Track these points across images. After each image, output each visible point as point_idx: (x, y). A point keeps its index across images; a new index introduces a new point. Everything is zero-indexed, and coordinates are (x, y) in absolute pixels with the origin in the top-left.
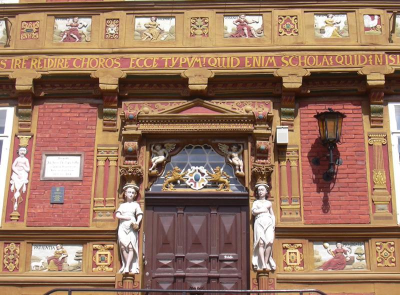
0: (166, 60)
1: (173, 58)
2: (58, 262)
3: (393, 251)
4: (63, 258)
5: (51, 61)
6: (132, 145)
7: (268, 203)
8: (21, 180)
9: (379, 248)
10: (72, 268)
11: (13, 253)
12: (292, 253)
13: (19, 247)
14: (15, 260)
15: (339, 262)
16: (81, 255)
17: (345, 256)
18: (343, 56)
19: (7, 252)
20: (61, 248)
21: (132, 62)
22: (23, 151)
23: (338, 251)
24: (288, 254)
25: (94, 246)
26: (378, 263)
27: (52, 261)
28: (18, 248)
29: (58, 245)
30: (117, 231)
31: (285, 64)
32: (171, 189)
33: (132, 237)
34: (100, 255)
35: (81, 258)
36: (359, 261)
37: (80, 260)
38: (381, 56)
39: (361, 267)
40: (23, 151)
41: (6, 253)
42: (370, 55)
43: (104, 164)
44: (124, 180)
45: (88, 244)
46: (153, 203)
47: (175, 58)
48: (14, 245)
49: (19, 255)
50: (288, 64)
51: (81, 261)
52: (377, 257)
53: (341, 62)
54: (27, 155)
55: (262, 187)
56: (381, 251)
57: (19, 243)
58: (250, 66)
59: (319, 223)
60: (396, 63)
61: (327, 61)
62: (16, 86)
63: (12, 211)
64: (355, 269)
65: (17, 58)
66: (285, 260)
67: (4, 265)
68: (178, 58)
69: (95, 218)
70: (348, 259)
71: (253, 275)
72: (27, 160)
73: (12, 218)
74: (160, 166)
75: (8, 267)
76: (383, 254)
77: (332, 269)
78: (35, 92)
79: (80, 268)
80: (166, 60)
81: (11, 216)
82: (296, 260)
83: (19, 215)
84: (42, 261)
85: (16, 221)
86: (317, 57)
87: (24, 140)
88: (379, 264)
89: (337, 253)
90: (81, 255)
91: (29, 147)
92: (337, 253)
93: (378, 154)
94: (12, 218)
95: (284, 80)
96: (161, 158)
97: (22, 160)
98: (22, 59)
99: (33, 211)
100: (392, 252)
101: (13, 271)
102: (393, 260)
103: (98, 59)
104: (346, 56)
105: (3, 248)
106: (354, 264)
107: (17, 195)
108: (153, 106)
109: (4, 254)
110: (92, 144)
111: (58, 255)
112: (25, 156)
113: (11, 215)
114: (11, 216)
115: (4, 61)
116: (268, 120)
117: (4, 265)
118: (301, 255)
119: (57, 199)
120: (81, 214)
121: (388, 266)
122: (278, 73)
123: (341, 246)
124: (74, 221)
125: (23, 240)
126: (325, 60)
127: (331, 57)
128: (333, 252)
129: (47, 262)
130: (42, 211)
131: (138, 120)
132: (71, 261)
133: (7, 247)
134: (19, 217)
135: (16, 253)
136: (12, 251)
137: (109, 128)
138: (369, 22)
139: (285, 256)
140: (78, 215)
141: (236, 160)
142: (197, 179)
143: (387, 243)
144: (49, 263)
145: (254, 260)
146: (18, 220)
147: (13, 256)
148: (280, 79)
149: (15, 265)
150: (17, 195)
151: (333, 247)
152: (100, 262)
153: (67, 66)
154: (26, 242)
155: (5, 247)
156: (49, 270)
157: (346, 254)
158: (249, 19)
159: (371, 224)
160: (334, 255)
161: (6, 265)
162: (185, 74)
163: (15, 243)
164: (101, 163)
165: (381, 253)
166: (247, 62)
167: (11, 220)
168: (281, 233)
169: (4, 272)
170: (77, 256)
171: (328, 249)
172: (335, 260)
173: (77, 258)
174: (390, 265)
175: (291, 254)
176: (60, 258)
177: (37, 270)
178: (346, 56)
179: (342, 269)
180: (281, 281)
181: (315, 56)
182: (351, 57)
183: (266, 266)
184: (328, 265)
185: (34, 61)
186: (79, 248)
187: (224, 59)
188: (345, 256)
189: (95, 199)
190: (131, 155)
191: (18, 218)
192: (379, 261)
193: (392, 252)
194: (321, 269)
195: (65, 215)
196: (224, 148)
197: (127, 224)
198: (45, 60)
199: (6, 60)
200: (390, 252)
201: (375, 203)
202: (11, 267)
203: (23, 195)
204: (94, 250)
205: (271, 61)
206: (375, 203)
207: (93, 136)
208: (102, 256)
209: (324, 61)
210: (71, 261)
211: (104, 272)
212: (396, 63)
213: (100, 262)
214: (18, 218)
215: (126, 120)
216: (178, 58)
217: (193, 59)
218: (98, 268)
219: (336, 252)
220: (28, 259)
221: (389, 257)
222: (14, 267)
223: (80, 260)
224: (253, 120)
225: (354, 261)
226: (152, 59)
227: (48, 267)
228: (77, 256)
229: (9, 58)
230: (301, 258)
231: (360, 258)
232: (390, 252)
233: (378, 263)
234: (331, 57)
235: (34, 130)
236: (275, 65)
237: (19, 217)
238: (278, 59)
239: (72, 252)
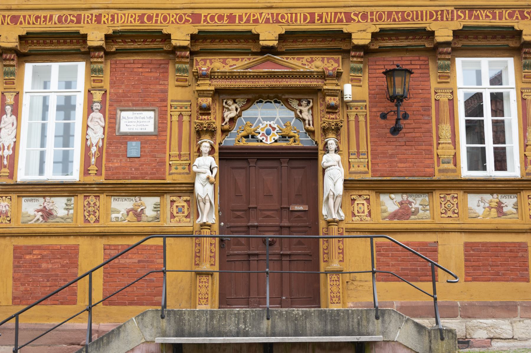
0: (237, 16)
1: (244, 14)
2: (138, 215)
3: (457, 202)
4: (142, 209)
5: (121, 16)
6: (206, 101)
7: (337, 157)
9: (443, 200)
10: (151, 219)
11: (93, 205)
12: (360, 203)
13: (99, 200)
14: (96, 212)
16: (159, 206)
17: (410, 207)
18: (412, 12)
19: (87, 205)
20: (140, 200)
21: (203, 18)
22: (97, 106)
23: (403, 203)
24: (356, 205)
25: (172, 198)
26: (442, 213)
27: (131, 213)
28: (98, 201)
29: (137, 198)
30: (193, 184)
31: (354, 20)
32: (244, 143)
33: (210, 188)
34: (177, 206)
35: (158, 209)
36: (423, 212)
37: (157, 211)
38: (450, 11)
39: (425, 218)
40: (97, 106)
41: (86, 206)
42: (438, 11)
43: (178, 120)
45: (165, 195)
47: (246, 14)
48: (94, 198)
49: (99, 207)
50: (357, 21)
51: (159, 212)
52: (441, 208)
53: (409, 18)
54: (102, 111)
55: (332, 143)
56: (444, 203)
57: (99, 196)
58: (320, 22)
59: (386, 175)
60: (465, 19)
61: (396, 17)
62: (88, 42)
63: (90, 166)
64: (419, 219)
65: (87, 13)
66: (353, 210)
67: (85, 216)
68: (248, 14)
69: (171, 172)
70: (413, 209)
72: (100, 115)
73: (90, 172)
74: (232, 120)
75: (89, 219)
76: (446, 205)
77: (398, 219)
78: (106, 46)
79: (158, 219)
80: (237, 16)
81: (89, 170)
82: (364, 210)
83: (97, 169)
84: (121, 213)
85: (94, 175)
86: (386, 13)
87: (98, 96)
88: (443, 215)
89: (402, 204)
90: (159, 206)
91: (103, 102)
92: (402, 204)
93: (446, 109)
94: (90, 172)
95: (354, 36)
96: (233, 114)
97: (97, 115)
98: (92, 15)
99: (111, 165)
100: (455, 203)
101: (94, 222)
102: (456, 211)
103: (169, 14)
104: (415, 13)
105: (83, 201)
106: (419, 214)
107: (94, 150)
108: (224, 62)
109: (84, 206)
110: (164, 100)
111: (137, 207)
112: (100, 111)
113: (88, 169)
114: (89, 170)
115: (73, 16)
116: (339, 75)
117: (85, 216)
118: (368, 206)
120: (157, 167)
121: (451, 217)
122: (346, 29)
123: (406, 198)
124: (151, 174)
125: (103, 193)
126: (394, 16)
127: (400, 13)
128: (399, 203)
129: (126, 213)
130: (119, 165)
131: (211, 76)
132: (149, 212)
133: (87, 200)
134: (97, 170)
135: (96, 205)
136: (92, 203)
137: (182, 83)
139: (353, 207)
140: (155, 168)
141: (306, 115)
142: (268, 133)
143: (452, 195)
144: (128, 215)
146: (96, 174)
147: (93, 208)
148: (349, 36)
149: (95, 217)
150: (94, 150)
151: (398, 198)
152: (177, 213)
153: (138, 21)
154: (105, 194)
155: (85, 200)
156: (129, 221)
157: (411, 205)
159: (436, 177)
160: (400, 206)
161: (87, 217)
162: (255, 29)
163: (94, 196)
164: (175, 118)
165: (445, 204)
166: (317, 18)
167: (90, 174)
169: (86, 224)
170: (155, 208)
171: (395, 200)
172: (401, 210)
173: (156, 209)
174: (452, 216)
175: (360, 205)
176: (139, 210)
177: (117, 221)
178: (415, 13)
179: (407, 219)
181: (384, 12)
182: (419, 12)
183: (335, 216)
184: (394, 216)
185: (105, 16)
186: (157, 200)
187: (294, 15)
188: (410, 207)
189: (170, 153)
190: (205, 111)
191: (96, 172)
192: (442, 212)
193: (455, 203)
194: (387, 219)
195: (142, 168)
196: (295, 104)
197: (204, 176)
198: (116, 16)
199: (76, 15)
200: (453, 204)
201: (439, 157)
202: (92, 218)
203: (100, 150)
204: (171, 201)
205: (341, 18)
206: (439, 157)
207: (165, 92)
208: (179, 207)
209: (393, 17)
210: (149, 212)
212: (465, 19)
213: (177, 213)
214: (96, 172)
215: (199, 76)
216: (248, 14)
217: (263, 15)
218: (175, 219)
219: (401, 203)
220: (109, 211)
221: (453, 208)
222: (95, 219)
223: (157, 211)
224: (323, 76)
225: (418, 212)
226: (223, 15)
227: (127, 219)
228: (155, 208)
229: (79, 13)
230: (368, 209)
231: (424, 209)
232: (453, 204)
233: (442, 213)
234: (400, 13)
235: (107, 86)
236: (345, 21)
237: (97, 170)
238: (347, 15)
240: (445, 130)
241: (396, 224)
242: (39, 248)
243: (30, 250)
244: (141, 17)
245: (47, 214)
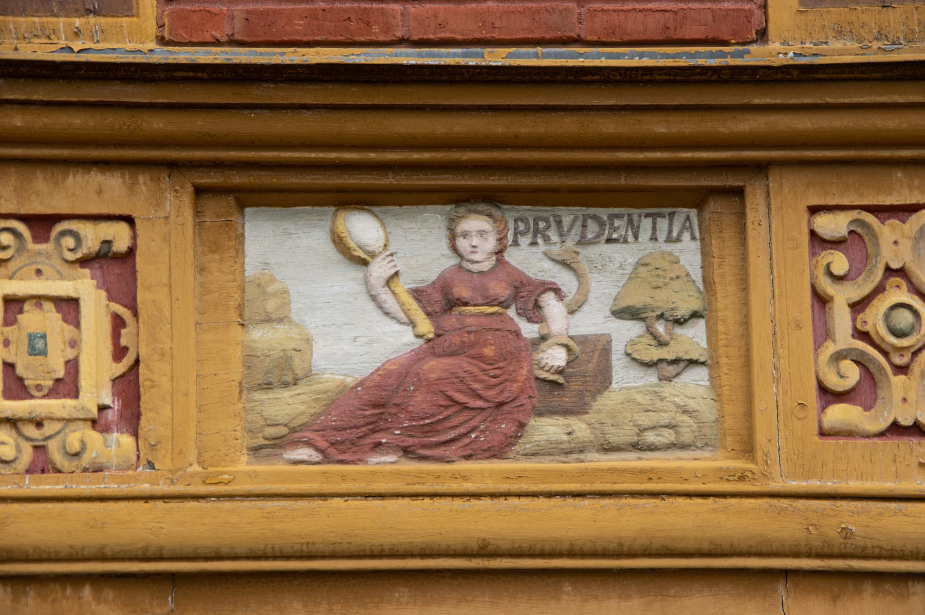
9: (840, 262)
12: (39, 299)
17: (529, 330)
23: (460, 291)
26: (828, 395)
36: (651, 378)
39: (668, 436)
52: (818, 346)
56: (855, 292)
64: (609, 448)
70: (556, 357)
76: (874, 318)
77: (407, 452)
82: (73, 366)
88: (838, 414)
89: (452, 303)
92: (452, 303)
106: (608, 401)
118: (118, 323)
123: (491, 244)
128: (418, 294)
157: (534, 313)
159: (774, 46)
160: (426, 327)
165: (858, 307)
171: (380, 270)
172: (434, 367)
179: (497, 452)
188: (529, 330)
192: (834, 382)
194: (304, 453)
225: (604, 378)
230: (119, 353)
231: (655, 354)
233: (828, 395)
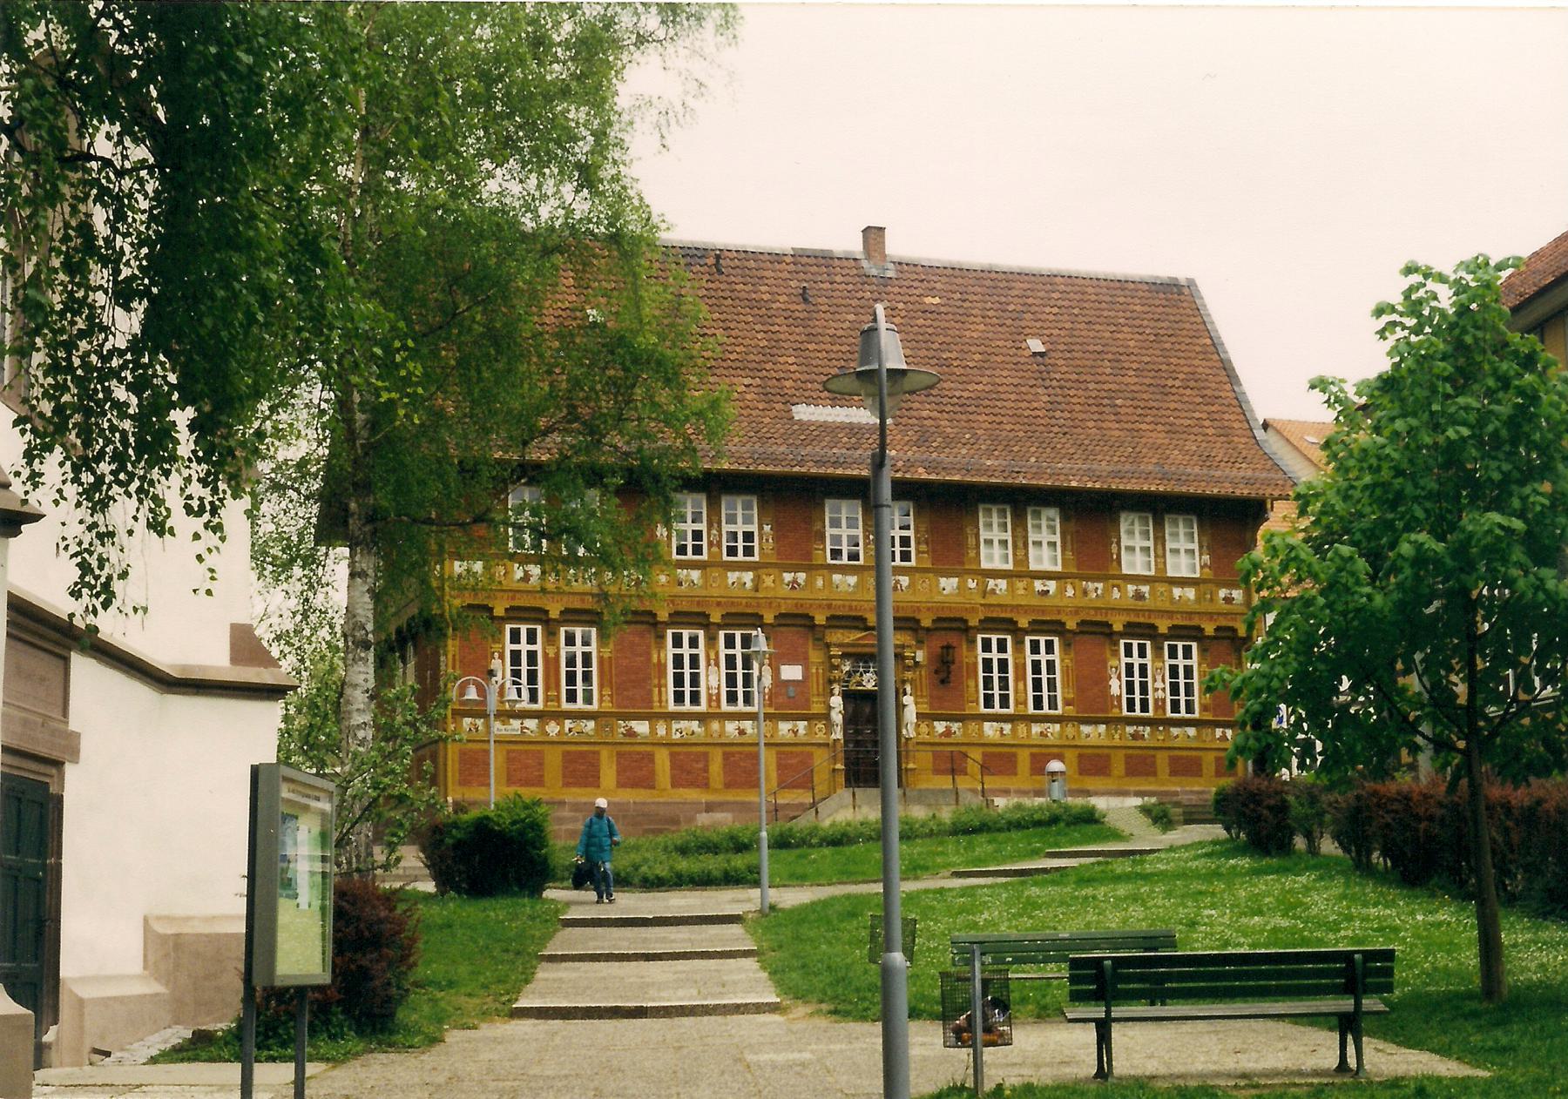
8: (767, 681)
15: (948, 733)
30: (829, 714)
44: (831, 682)
46: (847, 696)
71: (903, 740)
119: (792, 694)
132: (802, 732)
138: (972, 584)
145: (904, 732)
158: (900, 578)
168: (920, 716)
180: (918, 743)
207: (806, 653)
210: (802, 732)
211: (820, 737)
239: (802, 725)
240: (971, 683)
241: (944, 740)
242: (740, 753)
243: (733, 754)
244: (796, 605)
245: (742, 732)
